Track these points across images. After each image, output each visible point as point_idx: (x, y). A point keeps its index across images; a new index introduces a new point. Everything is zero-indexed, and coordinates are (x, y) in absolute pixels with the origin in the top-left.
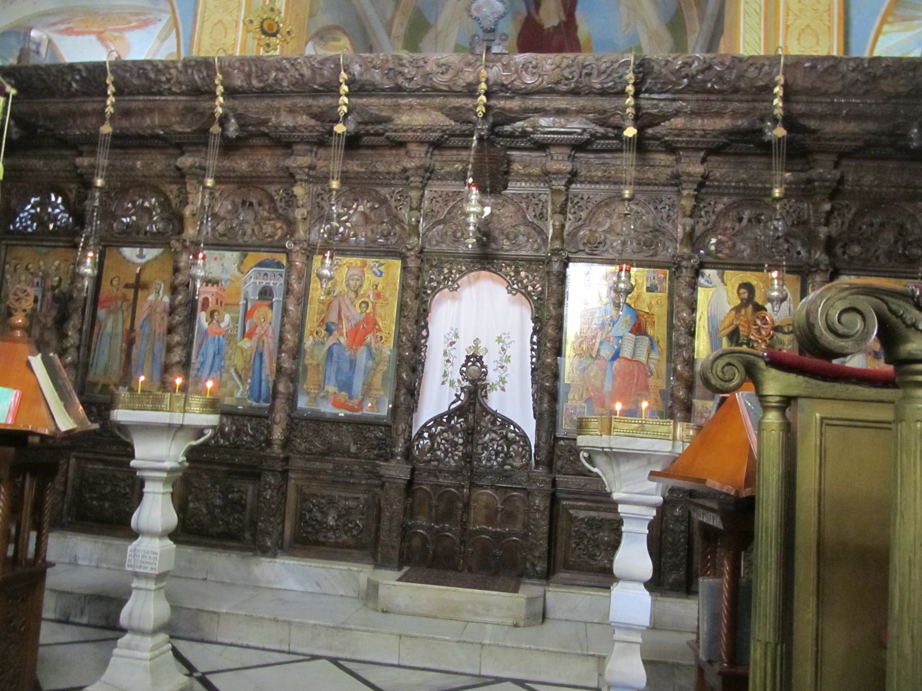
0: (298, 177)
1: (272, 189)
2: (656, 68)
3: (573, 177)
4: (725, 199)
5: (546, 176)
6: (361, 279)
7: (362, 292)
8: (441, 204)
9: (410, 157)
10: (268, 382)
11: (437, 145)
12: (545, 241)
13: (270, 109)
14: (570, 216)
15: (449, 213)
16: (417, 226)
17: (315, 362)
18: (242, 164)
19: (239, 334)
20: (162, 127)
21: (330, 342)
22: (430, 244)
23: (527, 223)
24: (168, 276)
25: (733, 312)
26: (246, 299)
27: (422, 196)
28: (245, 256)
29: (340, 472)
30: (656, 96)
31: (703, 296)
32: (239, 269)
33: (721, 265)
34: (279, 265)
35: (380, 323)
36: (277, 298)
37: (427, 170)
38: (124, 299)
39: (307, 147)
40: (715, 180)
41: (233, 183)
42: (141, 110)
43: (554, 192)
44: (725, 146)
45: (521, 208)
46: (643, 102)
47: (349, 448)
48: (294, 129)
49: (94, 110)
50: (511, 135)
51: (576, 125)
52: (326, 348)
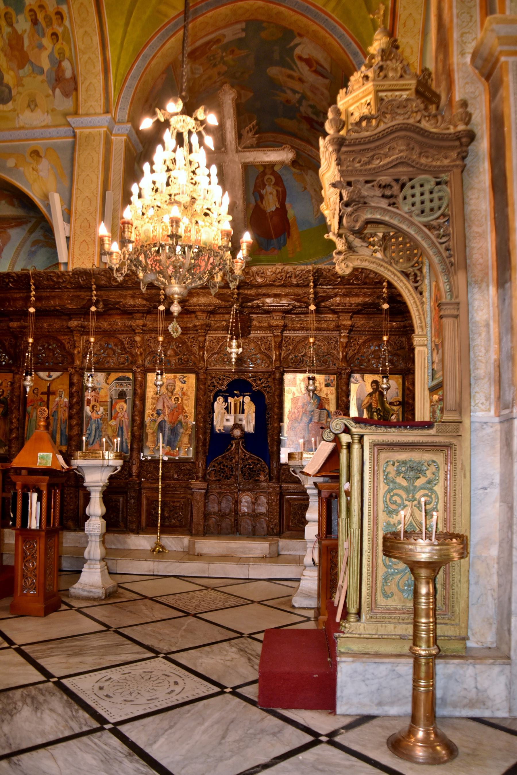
0: (137, 331)
1: (122, 337)
2: (325, 273)
3: (285, 327)
4: (363, 337)
5: (270, 328)
6: (174, 385)
7: (175, 392)
8: (215, 343)
9: (197, 319)
10: (127, 443)
11: (212, 313)
12: (271, 362)
13: (120, 296)
14: (284, 348)
15: (220, 348)
16: (203, 356)
17: (151, 431)
18: (105, 325)
19: (109, 417)
20: (59, 306)
21: (159, 420)
22: (210, 365)
23: (261, 352)
24: (66, 387)
25: (368, 397)
26: (111, 398)
27: (205, 340)
28: (109, 375)
29: (169, 489)
30: (325, 287)
31: (354, 388)
32: (106, 382)
33: (362, 372)
34: (128, 379)
35: (186, 409)
36: (129, 397)
37: (207, 326)
38: (42, 400)
39: (141, 315)
40: (358, 327)
41: (100, 334)
42: (48, 297)
43: (275, 336)
44: (362, 310)
45: (258, 344)
46: (318, 290)
47: (173, 475)
48: (135, 306)
49: (21, 297)
50: (252, 307)
51: (285, 302)
52: (157, 423)
